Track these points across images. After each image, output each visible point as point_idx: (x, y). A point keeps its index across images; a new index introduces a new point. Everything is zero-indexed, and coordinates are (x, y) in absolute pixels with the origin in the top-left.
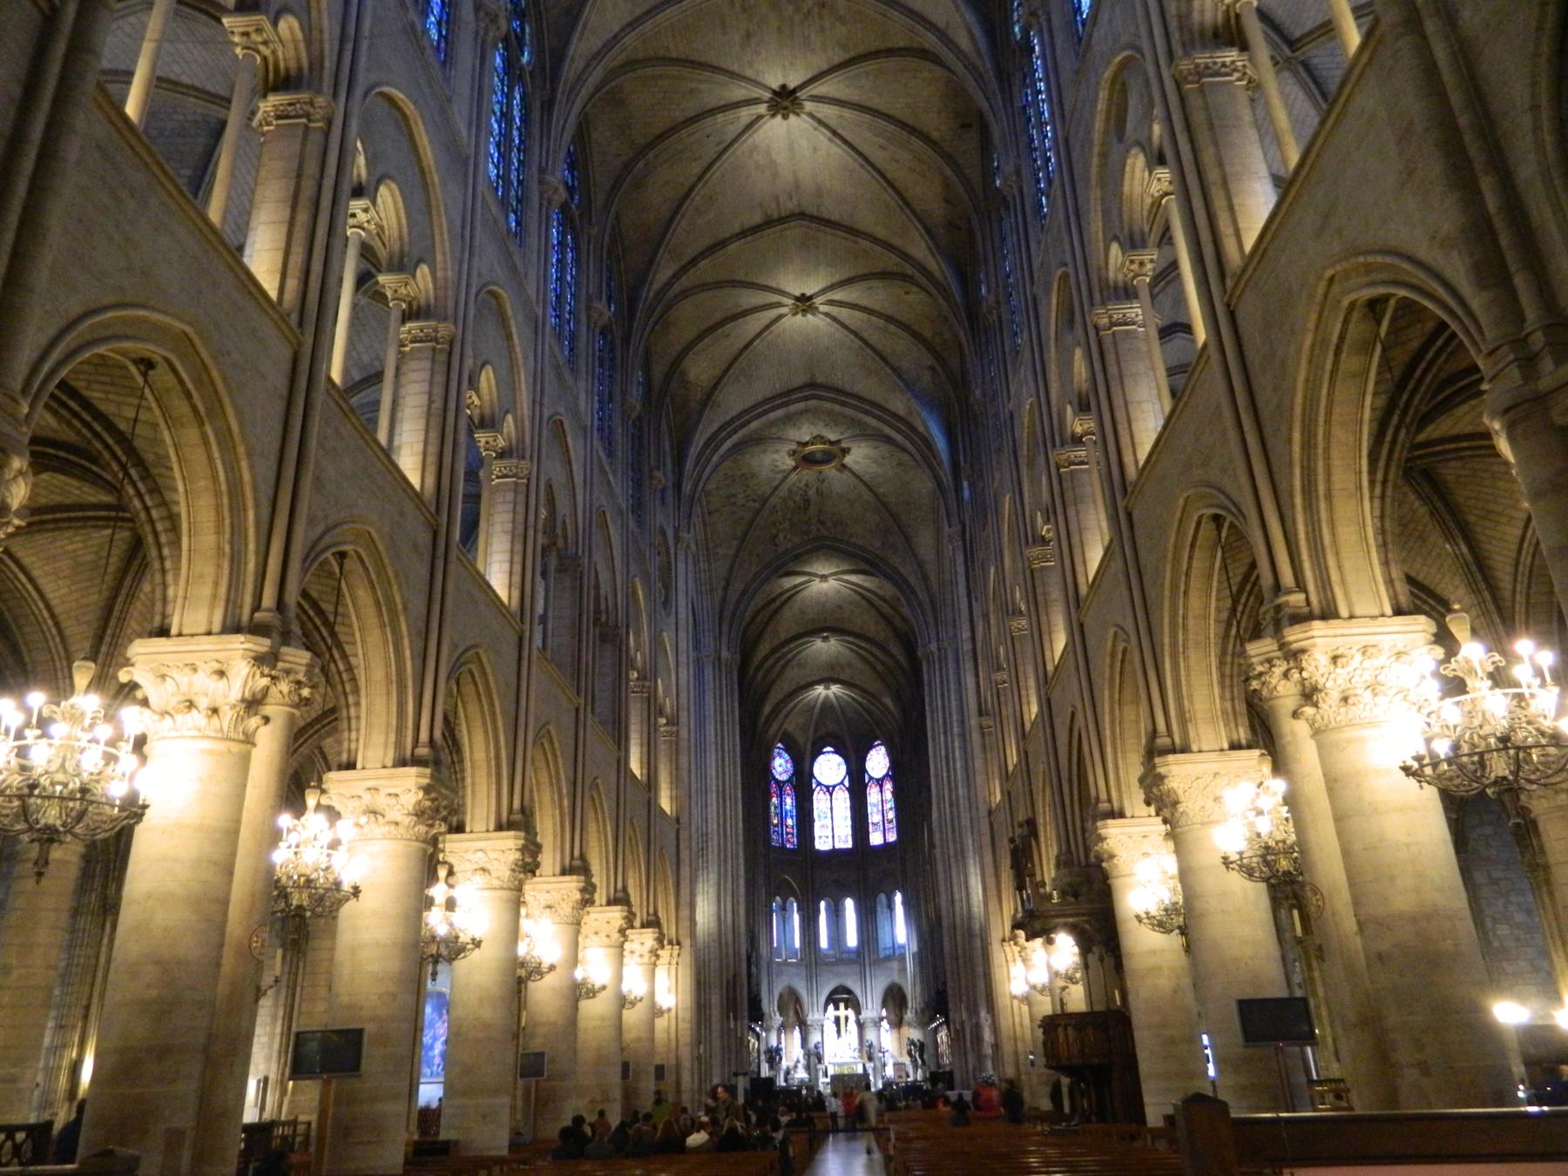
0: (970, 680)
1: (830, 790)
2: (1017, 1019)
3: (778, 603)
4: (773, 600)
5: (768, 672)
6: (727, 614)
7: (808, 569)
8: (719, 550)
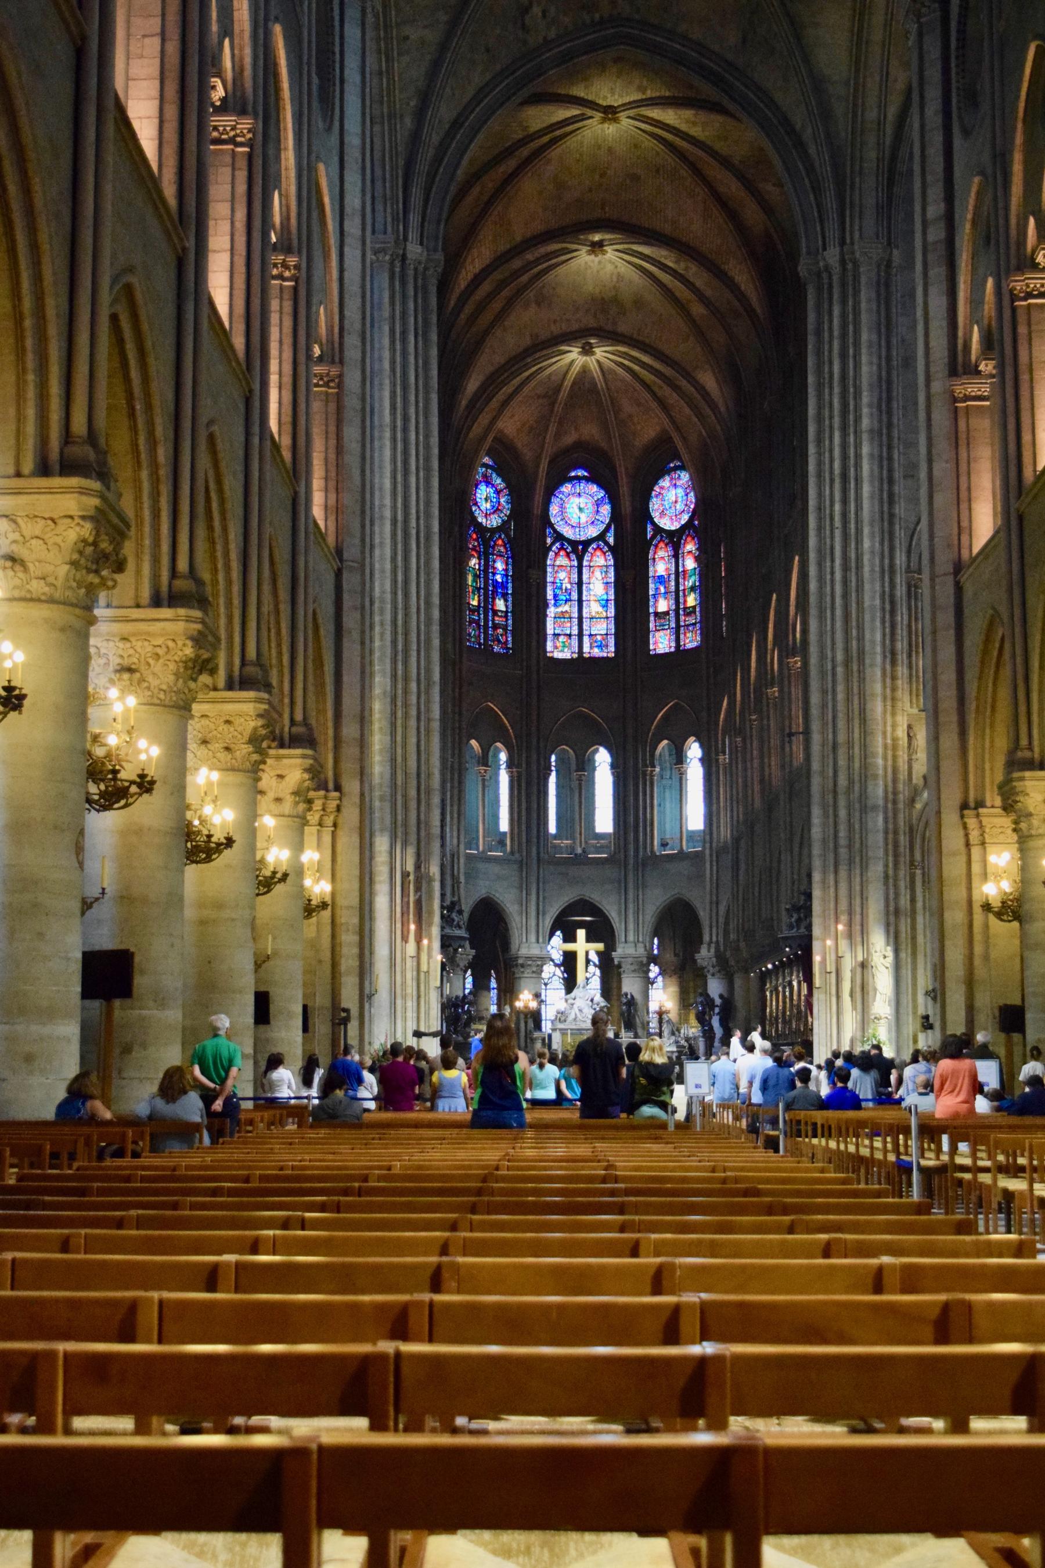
0: (938, 303)
1: (579, 549)
2: (978, 949)
3: (512, 163)
4: (508, 152)
5: (481, 307)
6: (422, 167)
7: (579, 91)
8: (407, 30)
